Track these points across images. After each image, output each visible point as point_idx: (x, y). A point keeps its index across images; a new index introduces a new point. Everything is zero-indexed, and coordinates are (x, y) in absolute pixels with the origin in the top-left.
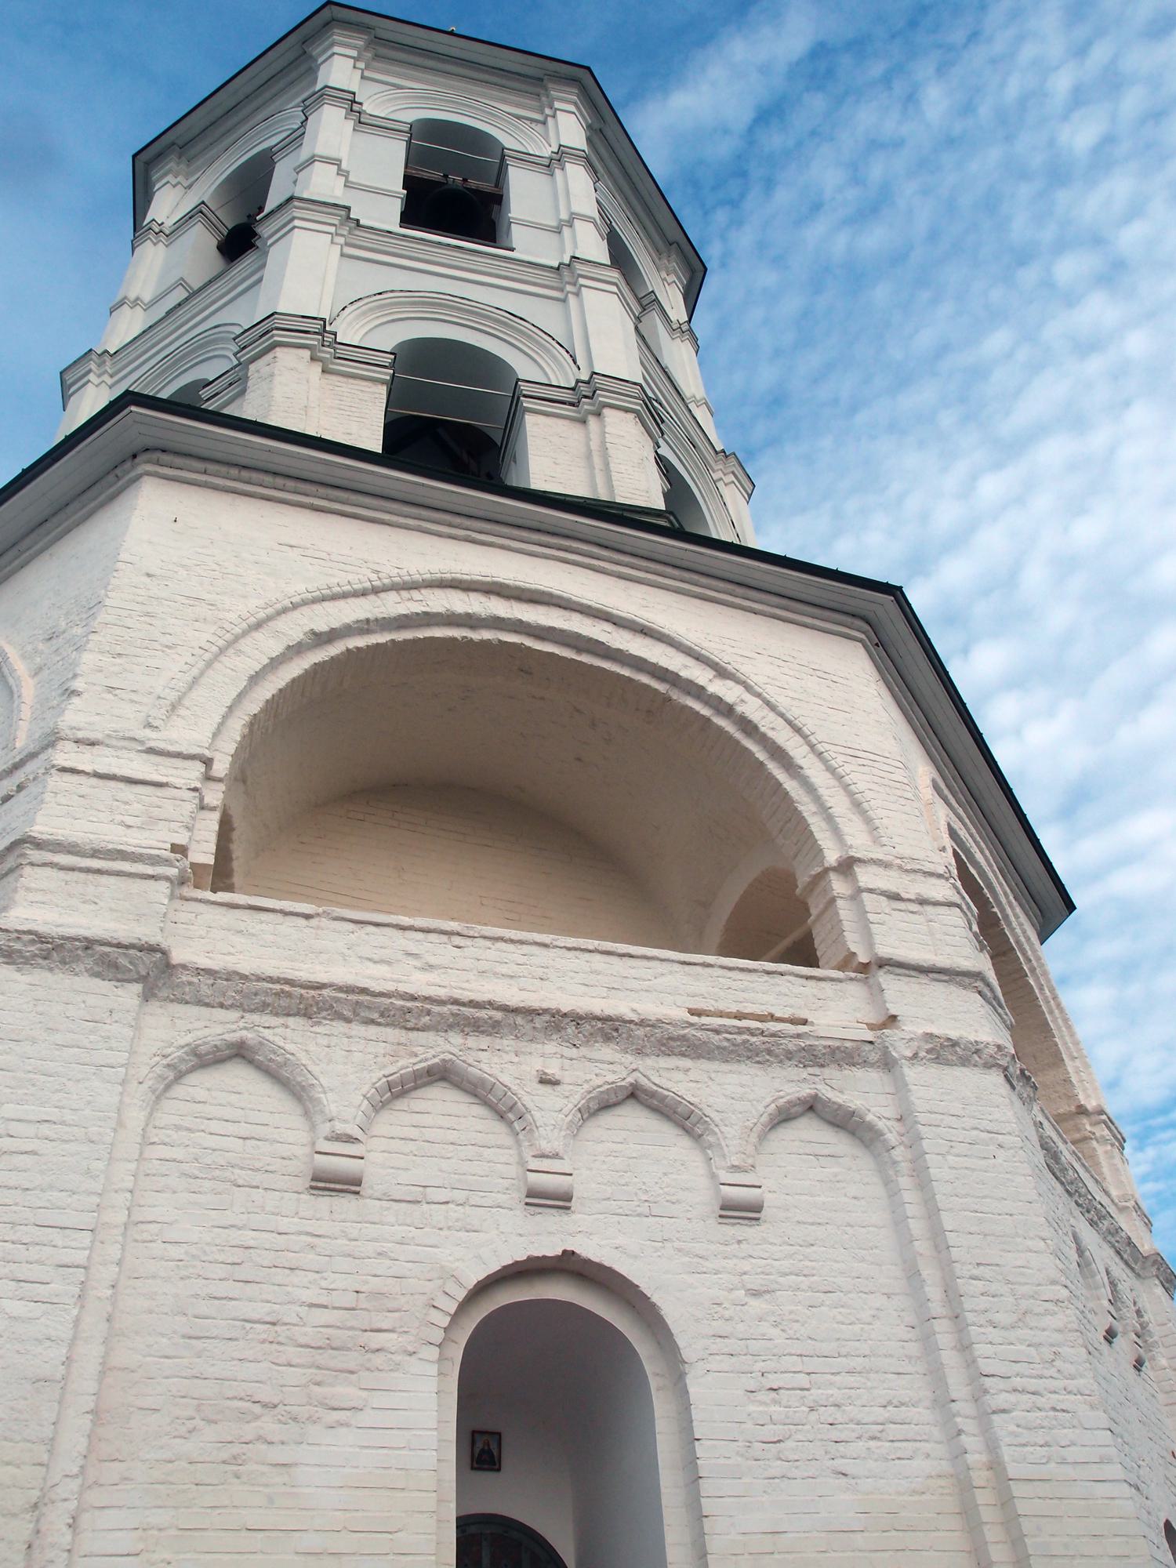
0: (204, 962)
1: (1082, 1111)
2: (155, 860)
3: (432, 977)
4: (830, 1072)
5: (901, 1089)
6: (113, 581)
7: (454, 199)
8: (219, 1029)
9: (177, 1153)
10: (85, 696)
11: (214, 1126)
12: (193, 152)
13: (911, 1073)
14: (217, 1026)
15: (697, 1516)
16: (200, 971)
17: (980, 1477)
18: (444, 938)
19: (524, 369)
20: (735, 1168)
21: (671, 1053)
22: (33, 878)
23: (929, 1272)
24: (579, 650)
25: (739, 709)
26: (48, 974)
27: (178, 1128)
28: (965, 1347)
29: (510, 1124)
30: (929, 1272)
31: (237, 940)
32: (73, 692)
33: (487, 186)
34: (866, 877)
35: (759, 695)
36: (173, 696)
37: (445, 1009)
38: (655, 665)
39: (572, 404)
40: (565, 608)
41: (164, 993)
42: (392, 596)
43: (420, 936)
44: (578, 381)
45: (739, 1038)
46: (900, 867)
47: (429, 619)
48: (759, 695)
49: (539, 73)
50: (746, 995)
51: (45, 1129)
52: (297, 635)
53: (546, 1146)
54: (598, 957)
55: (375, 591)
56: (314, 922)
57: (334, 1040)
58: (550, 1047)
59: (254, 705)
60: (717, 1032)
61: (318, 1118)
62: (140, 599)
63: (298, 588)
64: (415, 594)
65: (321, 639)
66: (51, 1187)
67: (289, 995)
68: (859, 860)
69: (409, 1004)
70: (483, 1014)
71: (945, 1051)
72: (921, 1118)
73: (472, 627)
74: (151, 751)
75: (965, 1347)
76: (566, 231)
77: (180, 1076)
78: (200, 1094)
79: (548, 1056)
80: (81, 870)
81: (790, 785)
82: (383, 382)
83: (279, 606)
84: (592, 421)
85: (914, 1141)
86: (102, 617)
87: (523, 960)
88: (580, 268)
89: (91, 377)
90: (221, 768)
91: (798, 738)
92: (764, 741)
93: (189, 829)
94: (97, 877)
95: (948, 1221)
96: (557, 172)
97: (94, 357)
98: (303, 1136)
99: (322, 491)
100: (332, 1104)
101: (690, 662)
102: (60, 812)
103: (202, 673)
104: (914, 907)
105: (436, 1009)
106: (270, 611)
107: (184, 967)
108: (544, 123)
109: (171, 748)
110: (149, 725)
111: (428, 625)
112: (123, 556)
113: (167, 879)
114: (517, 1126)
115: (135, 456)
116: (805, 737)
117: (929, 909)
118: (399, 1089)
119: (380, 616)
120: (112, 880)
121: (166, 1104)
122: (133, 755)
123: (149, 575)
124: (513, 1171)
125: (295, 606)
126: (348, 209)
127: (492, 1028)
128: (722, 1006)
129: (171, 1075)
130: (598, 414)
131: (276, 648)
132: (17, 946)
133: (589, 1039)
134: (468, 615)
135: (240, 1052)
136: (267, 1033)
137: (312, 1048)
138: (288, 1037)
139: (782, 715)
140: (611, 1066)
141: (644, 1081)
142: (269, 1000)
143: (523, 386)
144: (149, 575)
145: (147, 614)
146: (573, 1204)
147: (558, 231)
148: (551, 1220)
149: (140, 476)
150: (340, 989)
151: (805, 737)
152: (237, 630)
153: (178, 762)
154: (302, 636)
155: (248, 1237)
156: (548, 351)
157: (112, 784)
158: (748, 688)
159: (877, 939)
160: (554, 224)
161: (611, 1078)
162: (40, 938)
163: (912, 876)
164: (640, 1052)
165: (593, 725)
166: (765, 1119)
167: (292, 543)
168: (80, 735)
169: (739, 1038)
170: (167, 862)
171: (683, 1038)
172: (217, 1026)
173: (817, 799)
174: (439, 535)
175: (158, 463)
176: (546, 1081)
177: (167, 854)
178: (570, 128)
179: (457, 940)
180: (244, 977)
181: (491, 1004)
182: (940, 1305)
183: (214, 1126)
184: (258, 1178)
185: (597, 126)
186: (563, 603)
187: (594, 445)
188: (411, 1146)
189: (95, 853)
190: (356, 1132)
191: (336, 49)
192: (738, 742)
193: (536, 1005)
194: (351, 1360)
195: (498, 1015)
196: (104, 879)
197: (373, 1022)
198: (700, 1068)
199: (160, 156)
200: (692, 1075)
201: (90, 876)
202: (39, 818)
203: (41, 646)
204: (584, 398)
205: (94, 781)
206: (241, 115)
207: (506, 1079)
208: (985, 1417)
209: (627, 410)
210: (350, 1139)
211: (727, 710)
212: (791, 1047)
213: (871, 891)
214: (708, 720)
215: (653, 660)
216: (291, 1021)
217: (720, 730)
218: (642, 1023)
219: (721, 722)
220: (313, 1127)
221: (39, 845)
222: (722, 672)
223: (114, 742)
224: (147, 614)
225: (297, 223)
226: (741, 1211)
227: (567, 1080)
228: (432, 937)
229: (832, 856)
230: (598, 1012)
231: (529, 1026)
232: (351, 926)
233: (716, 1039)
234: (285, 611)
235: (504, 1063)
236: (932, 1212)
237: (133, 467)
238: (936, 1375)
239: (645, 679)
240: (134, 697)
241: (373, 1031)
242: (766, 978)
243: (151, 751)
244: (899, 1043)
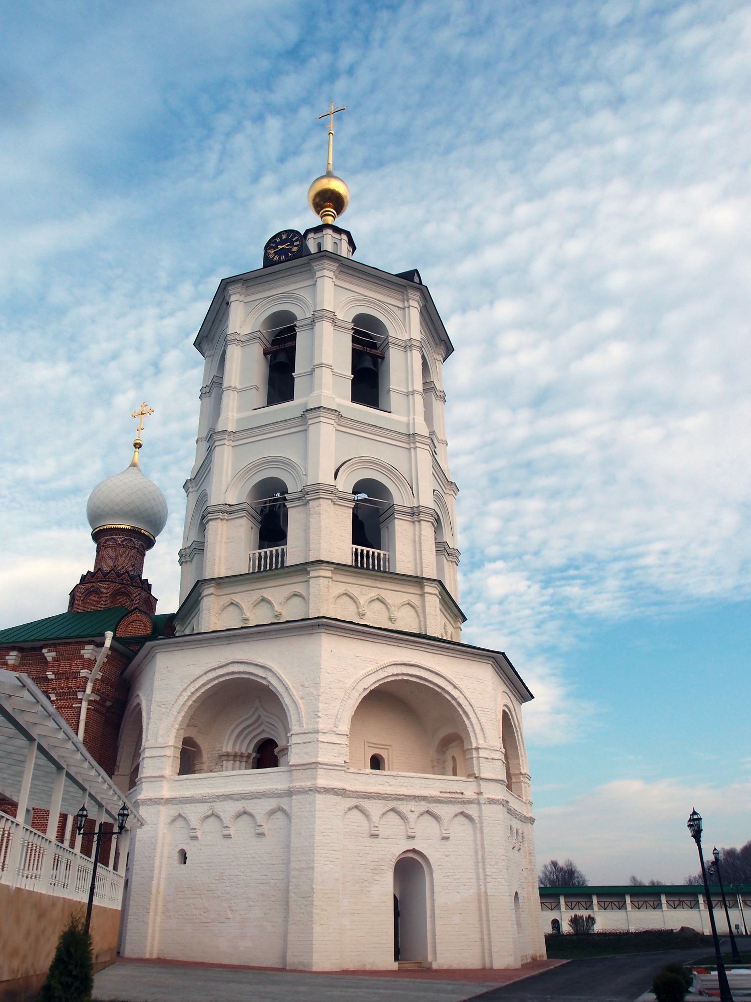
1: (521, 774)
4: (467, 806)
5: (480, 810)
14: (352, 802)
15: (433, 900)
17: (483, 894)
22: (320, 772)
23: (480, 853)
28: (484, 869)
30: (480, 853)
34: (482, 753)
42: (380, 672)
63: (362, 672)
71: (491, 801)
75: (484, 869)
79: (412, 805)
81: (467, 722)
85: (481, 823)
86: (322, 690)
95: (485, 843)
100: (374, 819)
101: (448, 683)
102: (325, 756)
127: (403, 799)
130: (419, 521)
138: (366, 804)
143: (396, 507)
148: (411, 841)
155: (360, 848)
176: (412, 811)
182: (481, 860)
194: (378, 871)
208: (485, 883)
211: (455, 699)
219: (453, 702)
222: (455, 687)
226: (445, 839)
236: (482, 840)
238: (478, 874)
244: (482, 799)
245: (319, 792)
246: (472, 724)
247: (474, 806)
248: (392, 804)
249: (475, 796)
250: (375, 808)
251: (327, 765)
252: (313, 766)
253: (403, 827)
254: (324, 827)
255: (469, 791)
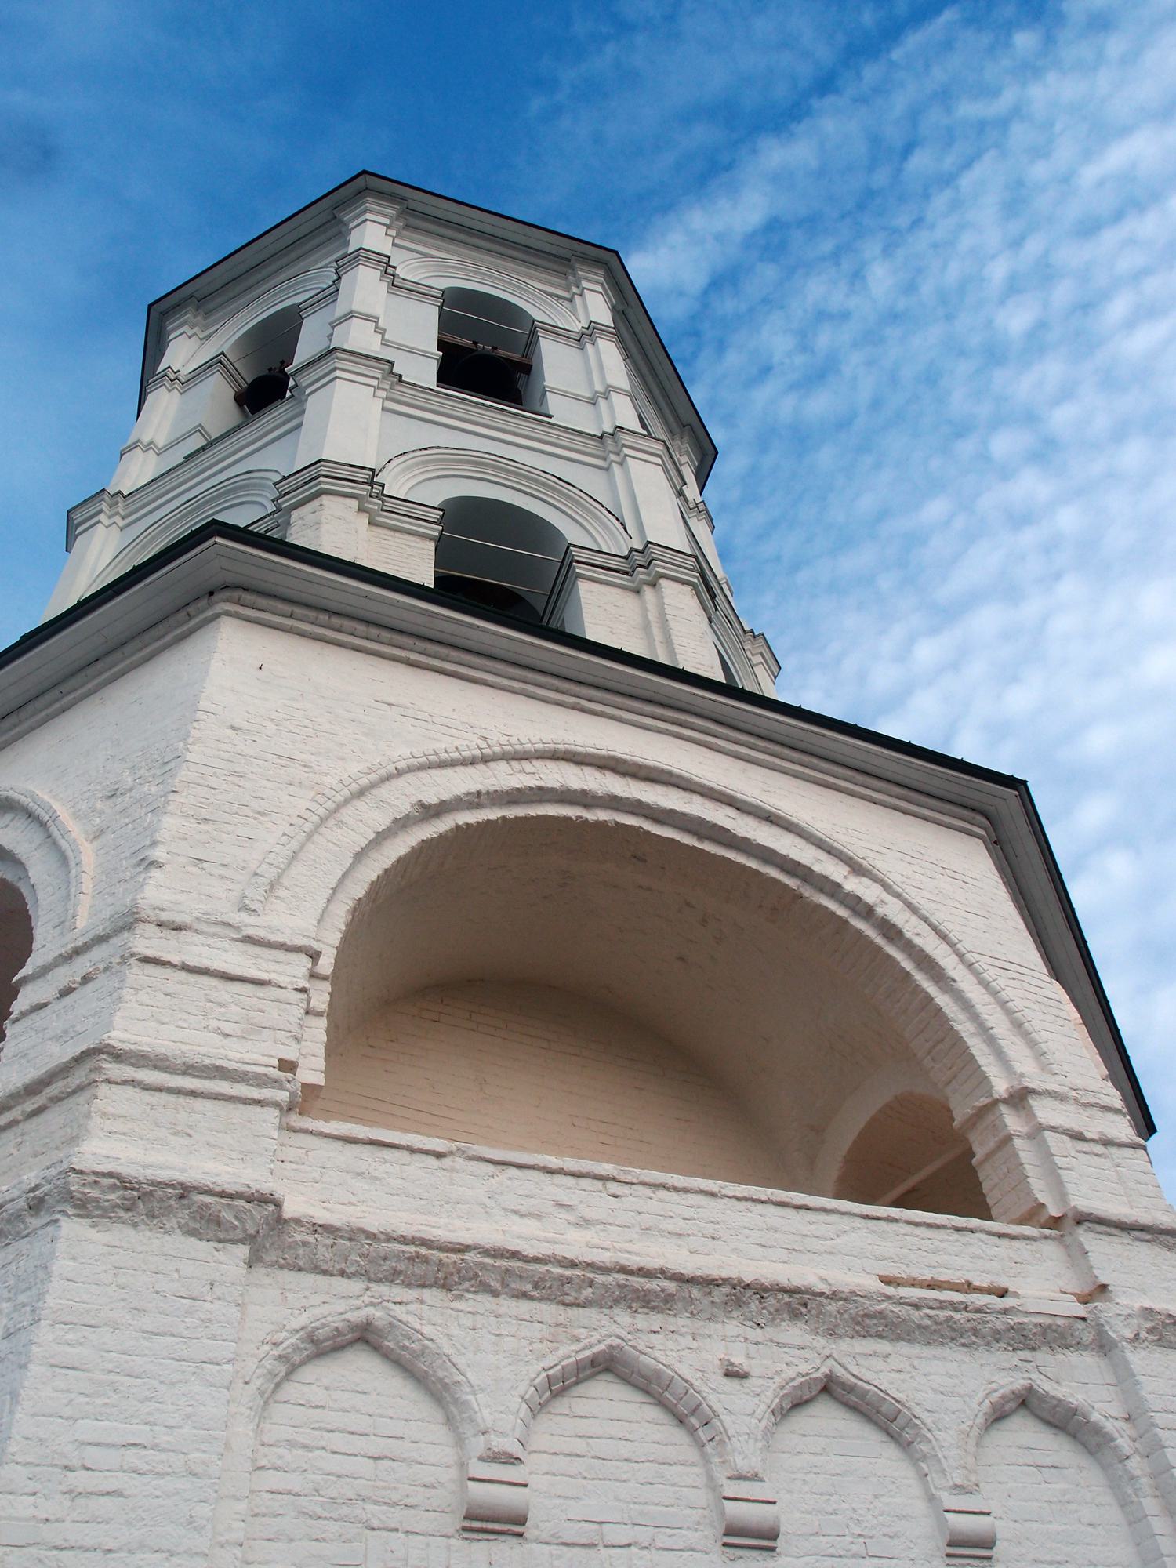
0: (322, 1216)
2: (262, 1081)
3: (589, 1235)
4: (1042, 1356)
5: (1125, 1380)
6: (193, 732)
7: (486, 363)
8: (341, 1306)
9: (294, 1482)
10: (168, 868)
11: (338, 1441)
12: (211, 305)
13: (1137, 1359)
14: (337, 1302)
16: (317, 1228)
18: (598, 1184)
19: (572, 534)
20: (959, 1489)
21: (866, 1334)
22: (108, 1098)
24: (701, 837)
25: (880, 911)
26: (131, 1232)
27: (291, 1444)
29: (692, 1432)
31: (359, 1185)
32: (152, 863)
33: (516, 356)
34: (1045, 1111)
35: (898, 896)
36: (271, 873)
37: (610, 1279)
38: (785, 857)
39: (626, 573)
40: (684, 789)
41: (271, 1257)
42: (502, 767)
43: (570, 1181)
44: (632, 550)
45: (943, 1314)
46: (1076, 1101)
47: (542, 794)
48: (898, 896)
49: (568, 254)
50: (937, 1258)
51: (132, 1457)
52: (404, 807)
53: (743, 1465)
54: (771, 1209)
55: (485, 760)
56: (447, 1162)
57: (480, 1321)
58: (732, 1328)
59: (358, 888)
60: (917, 1306)
61: (467, 1430)
62: (226, 756)
63: (402, 752)
64: (526, 765)
65: (430, 811)
66: (142, 1546)
67: (426, 1260)
68: (1033, 1092)
69: (569, 1273)
70: (654, 1285)
72: (1160, 1419)
73: (586, 806)
74: (249, 940)
76: (602, 402)
77: (293, 1369)
78: (317, 1395)
79: (728, 1339)
80: (171, 1091)
81: (942, 1000)
82: (431, 538)
83: (383, 772)
84: (648, 592)
85: (1153, 1449)
86: (183, 774)
87: (689, 1213)
88: (625, 438)
89: (102, 517)
90: (326, 965)
91: (944, 946)
92: (909, 947)
93: (298, 1040)
94: (190, 1100)
96: (589, 346)
97: (106, 497)
98: (446, 1453)
99: (421, 645)
102: (144, 1015)
103: (302, 846)
104: (1098, 1149)
105: (600, 1278)
106: (373, 777)
107: (298, 1221)
108: (571, 300)
109: (273, 938)
110: (245, 908)
111: (540, 801)
112: (203, 705)
113: (276, 1105)
114: (703, 1434)
115: (211, 594)
116: (952, 945)
117: (1114, 1150)
118: (559, 1386)
119: (492, 789)
120: (209, 1105)
121: (278, 1411)
122: (226, 944)
123: (233, 728)
124: (702, 1497)
125: (400, 773)
126: (392, 363)
128: (915, 1272)
129: (282, 1369)
130: (654, 585)
131: (382, 821)
132: (95, 1193)
133: (775, 1316)
134: (584, 792)
135: (364, 1337)
136: (398, 1311)
137: (455, 1331)
138: (427, 1317)
139: (925, 920)
140: (795, 1353)
141: (839, 1371)
142: (401, 1266)
143: (575, 551)
144: (233, 728)
145: (235, 774)
146: (780, 1543)
147: (593, 402)
149: (217, 616)
150: (487, 1252)
151: (952, 945)
152: (339, 798)
153: (280, 955)
154: (410, 809)
156: (597, 518)
157: (205, 980)
158: (886, 887)
159: (1070, 1188)
160: (588, 395)
161: (804, 1368)
162: (123, 1183)
163: (1090, 1111)
164: (832, 1333)
165: (704, 922)
166: (980, 1420)
167: (392, 701)
168: (164, 916)
169: (943, 1314)
170: (276, 1083)
171: (880, 1315)
172: (337, 1302)
173: (975, 1018)
174: (546, 701)
175: (239, 603)
176: (734, 1374)
177: (275, 1073)
178: (597, 307)
179: (614, 1187)
180: (371, 1236)
181: (663, 1273)
183: (338, 1441)
184: (395, 1517)
185: (620, 308)
186: (683, 784)
187: (652, 616)
188: (577, 1466)
189: (188, 1070)
190: (516, 1450)
191: (368, 216)
192: (880, 948)
193: (715, 1273)
195: (671, 1286)
196: (199, 1104)
197: (525, 1295)
198: (902, 1353)
199: (177, 308)
200: (895, 1362)
201: (182, 1100)
202: (118, 1020)
203: (99, 805)
204: (638, 567)
205: (183, 975)
206: (265, 272)
207: (686, 1371)
209: (683, 582)
210: (512, 1460)
211: (867, 912)
212: (999, 1326)
213: (1053, 1129)
214: (845, 922)
215: (784, 852)
216: (427, 1294)
217: (859, 933)
218: (834, 1296)
219: (859, 924)
220: (460, 1441)
221: (118, 1056)
222: (857, 868)
223: (204, 927)
224: (235, 774)
225: (338, 373)
227: (755, 1371)
228: (585, 1183)
229: (1001, 1086)
230: (784, 1283)
231: (706, 1301)
232: (491, 1168)
233: (916, 1315)
234: (389, 777)
235: (684, 1349)
237: (210, 605)
239: (773, 873)
240: (224, 871)
241: (524, 1307)
242: (956, 1236)
243: (249, 940)
245: (84, 1207)
246: (967, 1006)
247: (1085, 1362)
248: (602, 1329)
249: (1080, 1310)
250: (498, 1349)
251: (159, 1063)
252: (79, 1077)
253: (694, 1474)
254: (88, 1429)
255: (1039, 1280)
